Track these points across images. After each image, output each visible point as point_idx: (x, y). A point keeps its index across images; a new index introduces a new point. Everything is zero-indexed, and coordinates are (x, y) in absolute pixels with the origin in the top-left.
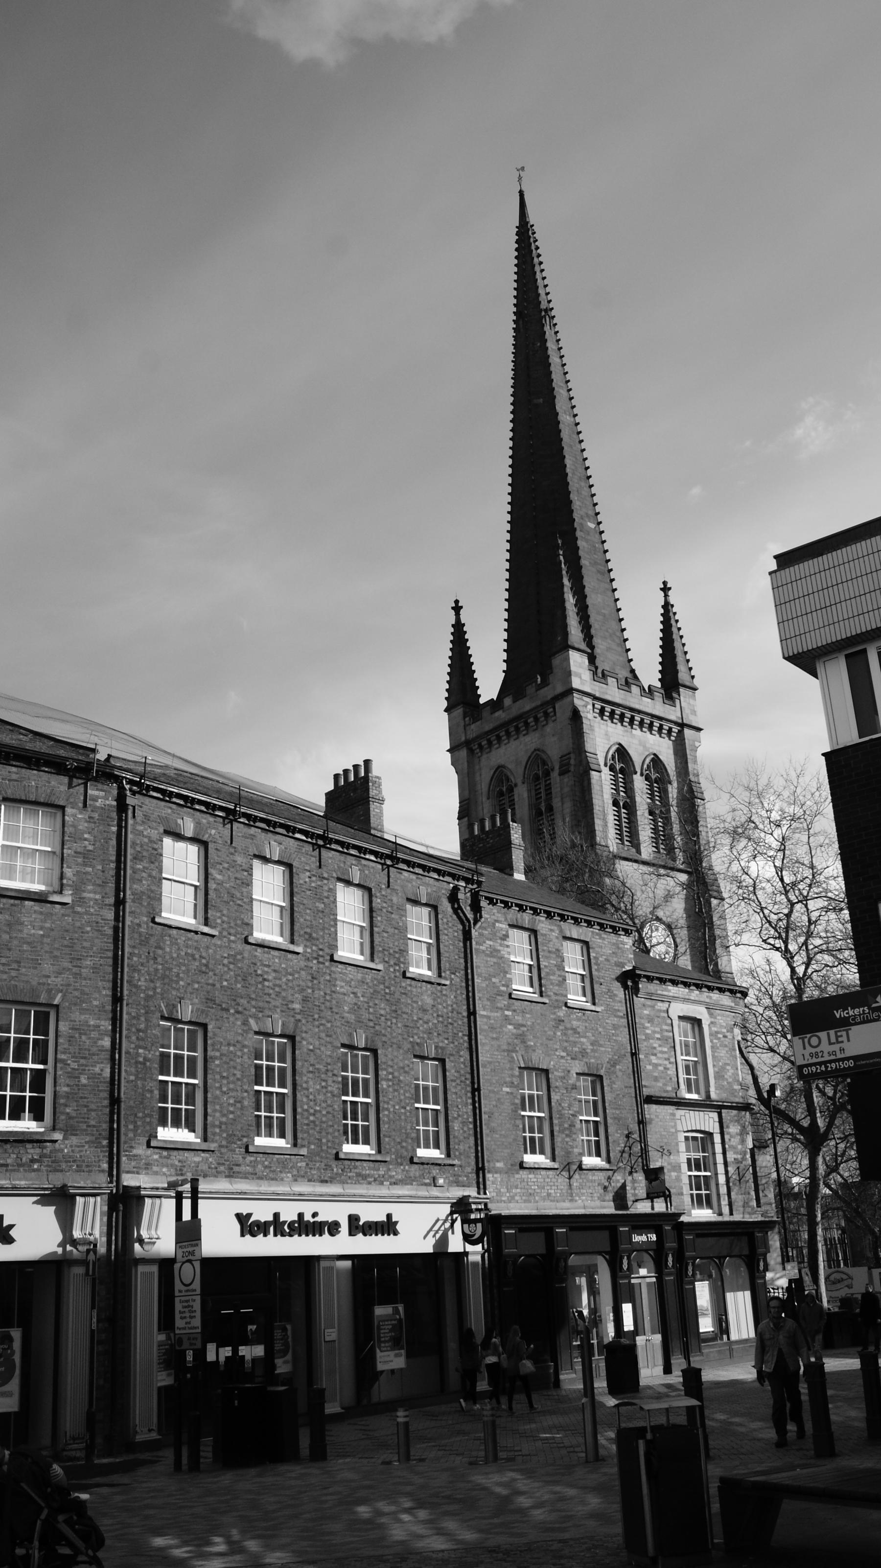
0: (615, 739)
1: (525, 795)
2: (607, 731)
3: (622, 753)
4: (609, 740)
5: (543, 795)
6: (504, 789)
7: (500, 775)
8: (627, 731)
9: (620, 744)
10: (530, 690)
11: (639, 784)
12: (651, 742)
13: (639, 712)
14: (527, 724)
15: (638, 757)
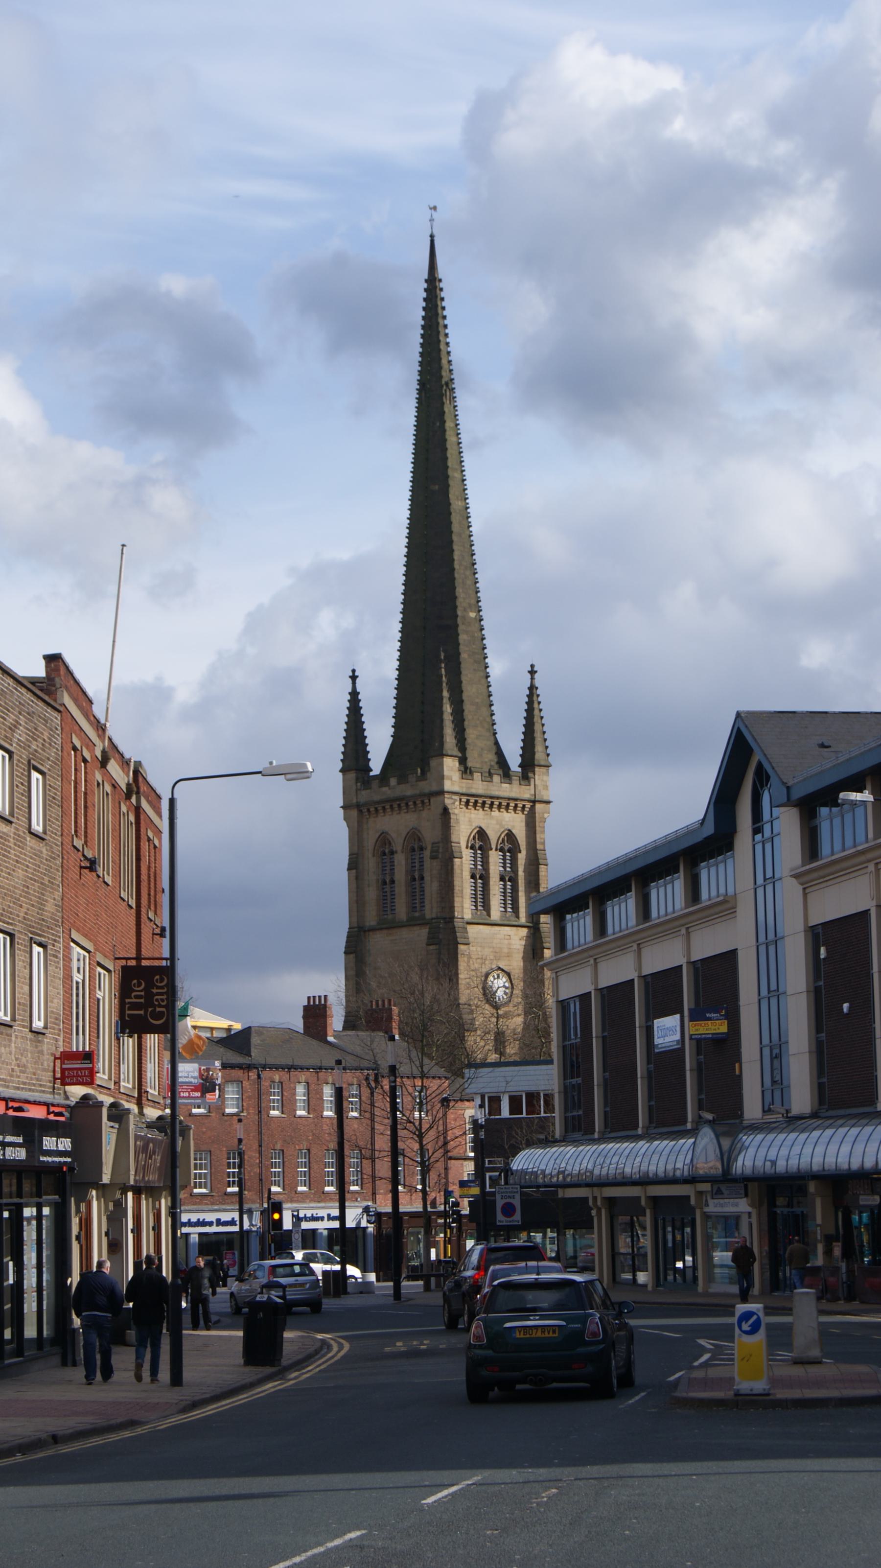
0: (475, 825)
1: (403, 862)
2: (470, 818)
3: (481, 834)
4: (471, 825)
5: (417, 865)
6: (387, 851)
7: (384, 840)
8: (487, 814)
9: (480, 828)
10: (412, 779)
11: (495, 858)
12: (507, 819)
13: (498, 798)
14: (407, 805)
15: (494, 835)
